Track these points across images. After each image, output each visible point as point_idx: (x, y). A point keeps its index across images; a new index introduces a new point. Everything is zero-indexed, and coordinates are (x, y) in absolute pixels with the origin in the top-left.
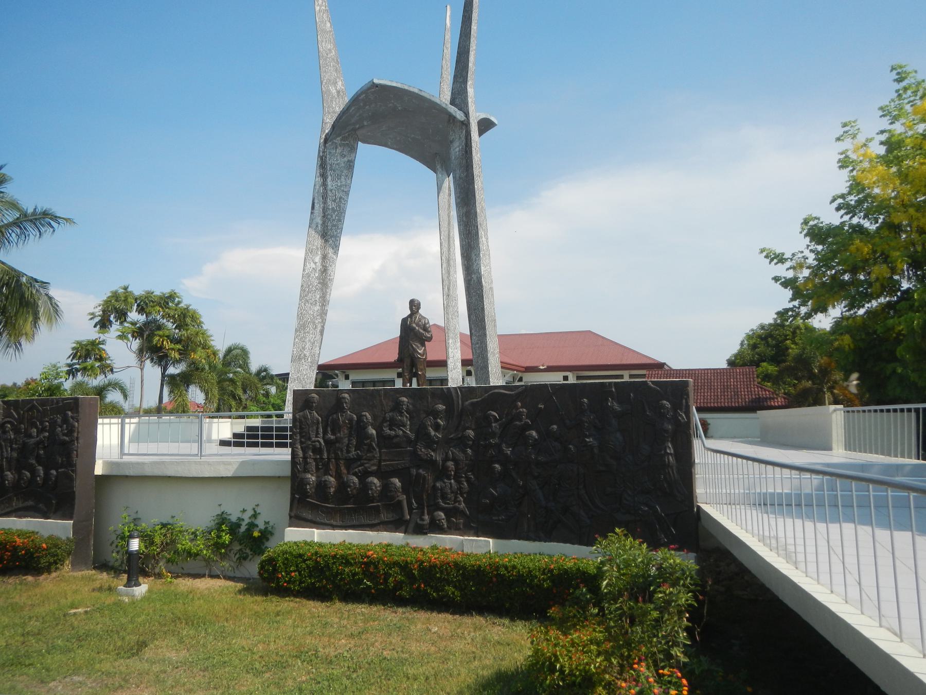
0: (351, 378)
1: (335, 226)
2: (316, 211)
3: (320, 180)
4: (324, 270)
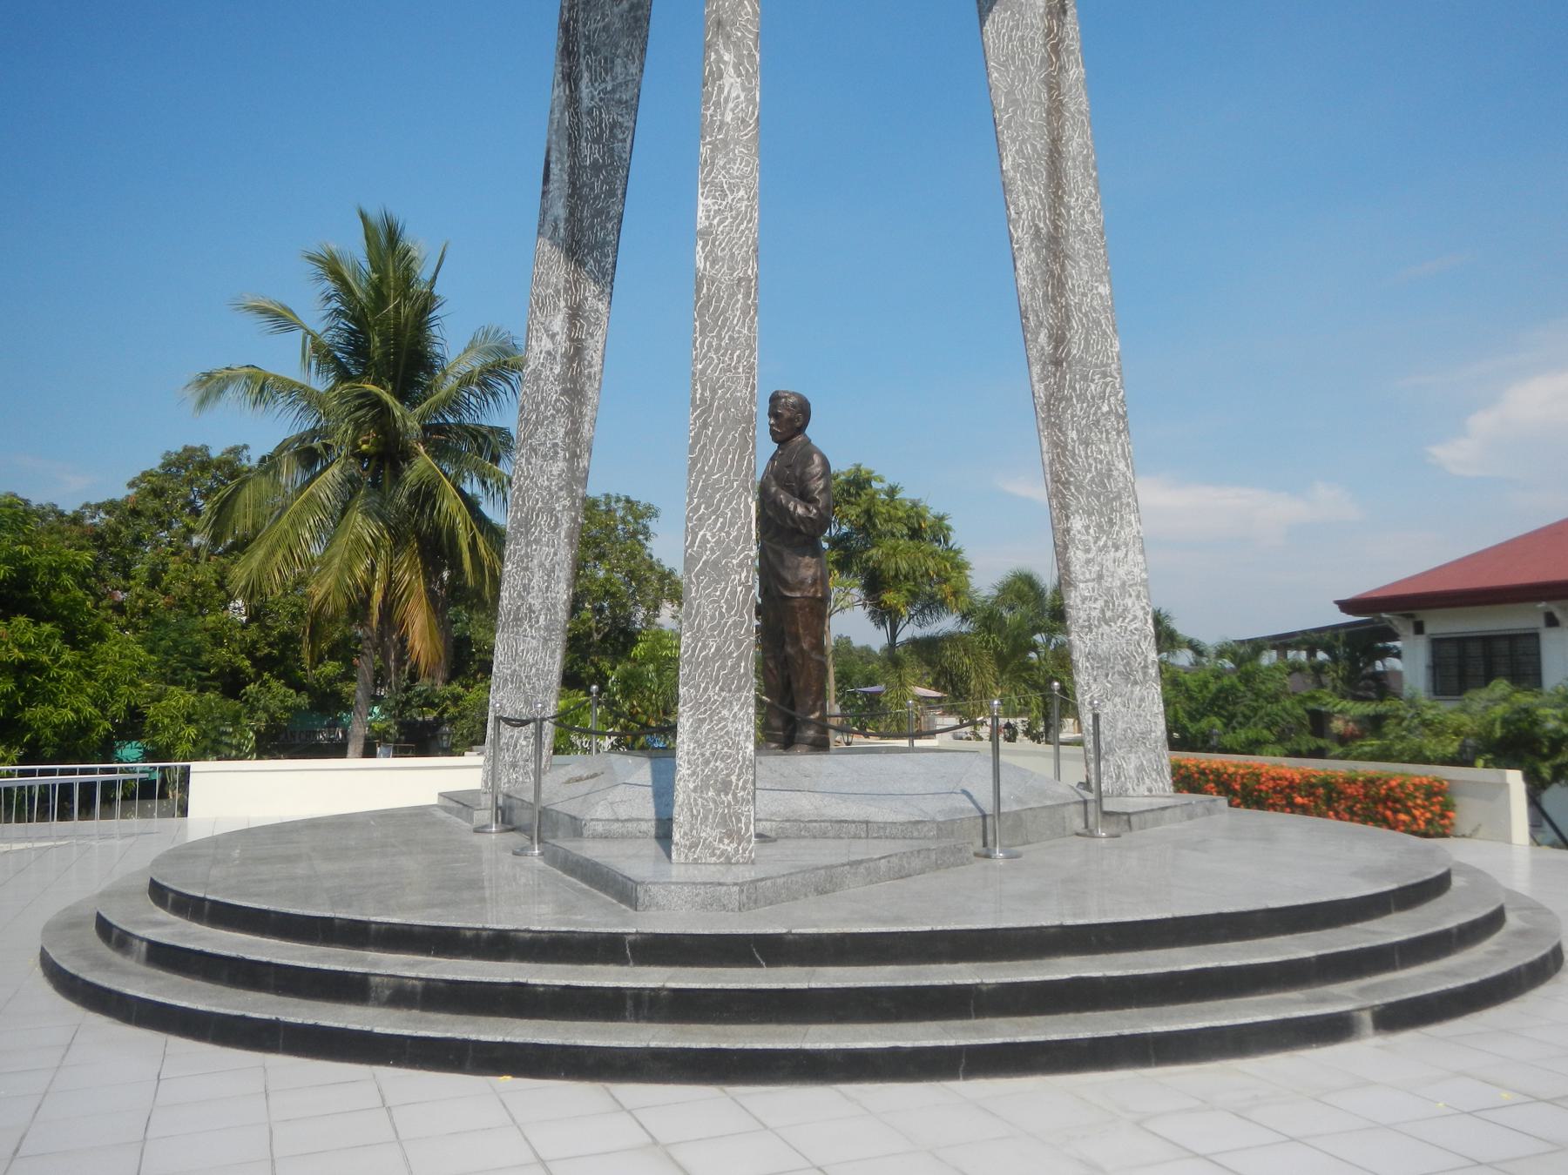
0: (1430, 628)
1: (598, 213)
2: (553, 186)
3: (561, 92)
4: (576, 352)
